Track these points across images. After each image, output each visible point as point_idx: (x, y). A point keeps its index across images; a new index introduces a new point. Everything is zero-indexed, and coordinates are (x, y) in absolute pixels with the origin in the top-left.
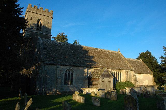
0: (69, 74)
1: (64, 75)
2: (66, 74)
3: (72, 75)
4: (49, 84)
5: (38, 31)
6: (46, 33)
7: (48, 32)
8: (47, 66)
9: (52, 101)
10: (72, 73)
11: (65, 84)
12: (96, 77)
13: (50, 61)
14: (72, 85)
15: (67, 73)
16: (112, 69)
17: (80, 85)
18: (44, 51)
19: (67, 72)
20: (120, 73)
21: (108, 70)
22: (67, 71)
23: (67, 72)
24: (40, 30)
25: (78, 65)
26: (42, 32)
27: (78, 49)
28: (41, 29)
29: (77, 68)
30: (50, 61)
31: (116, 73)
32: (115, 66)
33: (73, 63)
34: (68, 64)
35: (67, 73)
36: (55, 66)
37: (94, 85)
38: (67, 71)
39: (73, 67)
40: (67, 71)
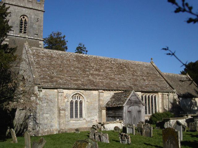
0: (76, 102)
1: (69, 103)
2: (72, 103)
3: (81, 103)
4: (47, 118)
5: (22, 35)
6: (35, 37)
7: (37, 35)
8: (44, 91)
9: (7, 133)
10: (81, 100)
11: (71, 118)
12: (119, 104)
13: (47, 82)
14: (81, 119)
15: (74, 101)
16: (142, 92)
17: (93, 118)
18: (37, 68)
19: (73, 99)
20: (155, 97)
21: (136, 93)
22: (73, 97)
23: (73, 99)
24: (25, 33)
25: (91, 88)
26: (29, 36)
27: (88, 62)
28: (26, 30)
29: (88, 92)
30: (47, 82)
31: (149, 97)
32: (146, 87)
33: (82, 85)
34: (73, 86)
35: (74, 101)
36: (56, 90)
37: (116, 116)
38: (74, 97)
39: (82, 91)
40: (74, 97)
